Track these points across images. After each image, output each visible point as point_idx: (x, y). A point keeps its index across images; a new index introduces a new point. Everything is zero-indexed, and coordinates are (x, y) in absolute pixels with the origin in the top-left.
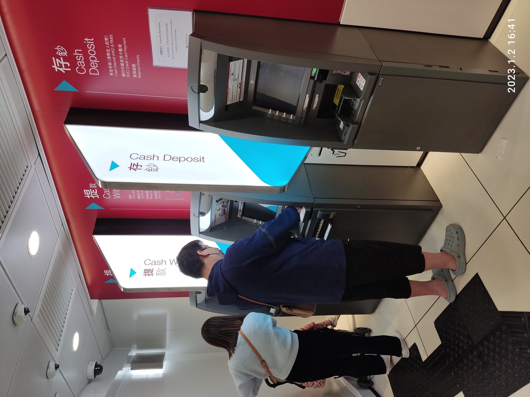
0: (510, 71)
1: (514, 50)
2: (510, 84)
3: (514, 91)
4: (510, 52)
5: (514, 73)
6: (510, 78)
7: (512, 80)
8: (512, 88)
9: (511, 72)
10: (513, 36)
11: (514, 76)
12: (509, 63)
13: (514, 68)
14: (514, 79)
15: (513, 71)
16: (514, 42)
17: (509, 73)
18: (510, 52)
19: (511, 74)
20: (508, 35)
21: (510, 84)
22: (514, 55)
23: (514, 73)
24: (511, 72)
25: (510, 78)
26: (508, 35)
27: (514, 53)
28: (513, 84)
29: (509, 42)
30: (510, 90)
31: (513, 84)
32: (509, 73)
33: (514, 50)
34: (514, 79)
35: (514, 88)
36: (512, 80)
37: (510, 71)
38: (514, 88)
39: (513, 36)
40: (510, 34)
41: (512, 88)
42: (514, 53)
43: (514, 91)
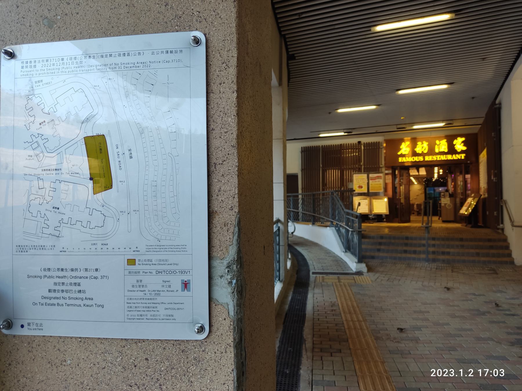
1: (473, 376)
2: (439, 372)
3: (432, 375)
4: (471, 371)
5: (450, 375)
6: (446, 371)
7: (444, 373)
8: (436, 374)
9: (451, 373)
11: (447, 376)
12: (460, 371)
13: (455, 375)
14: (444, 375)
15: (452, 374)
17: (450, 370)
18: (471, 371)
19: (449, 373)
21: (439, 372)
22: (468, 375)
23: (450, 375)
24: (451, 373)
25: (446, 371)
27: (470, 375)
28: (439, 374)
29: (480, 370)
30: (433, 371)
31: (439, 374)
32: (450, 370)
33: (473, 376)
34: (444, 375)
35: (435, 376)
36: (444, 373)
38: (435, 376)
41: (436, 374)
42: (470, 375)
43: (432, 375)
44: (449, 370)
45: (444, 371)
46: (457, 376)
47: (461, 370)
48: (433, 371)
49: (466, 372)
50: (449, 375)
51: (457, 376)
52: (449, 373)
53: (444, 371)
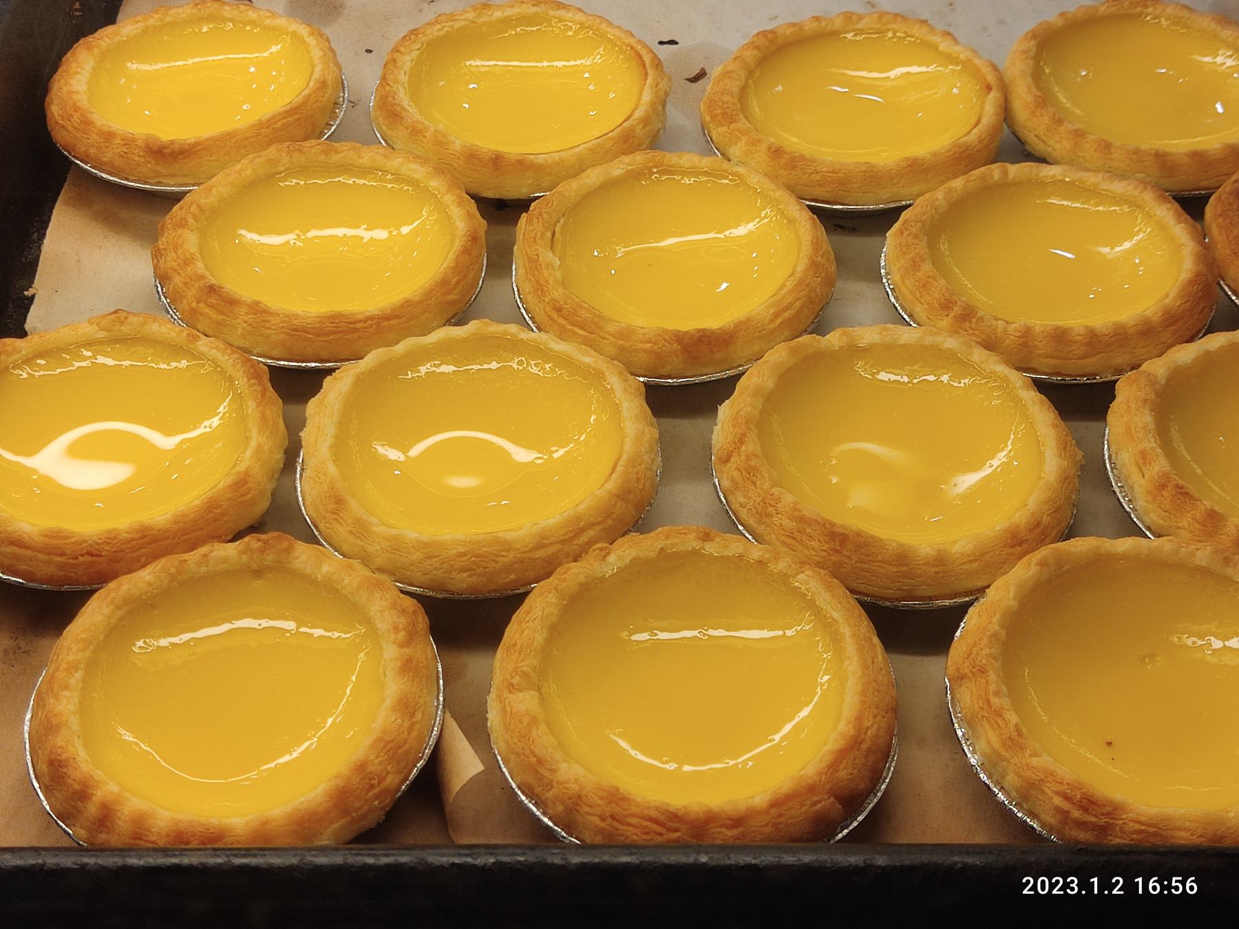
0: (1072, 882)
1: (1122, 893)
2: (1043, 882)
3: (1025, 892)
4: (1118, 882)
5: (1068, 891)
6: (1058, 882)
7: (1052, 886)
8: (1034, 888)
9: (1071, 885)
10: (1154, 888)
11: (1062, 893)
12: (1091, 880)
13: (1080, 891)
14: (1054, 892)
15: (1073, 889)
16: (1140, 892)
17: (1069, 880)
18: (1118, 882)
19: (1066, 886)
20: (1156, 878)
21: (1043, 882)
22: (1110, 892)
23: (1068, 891)
24: (1071, 885)
25: (1058, 882)
26: (1156, 878)
27: (1115, 892)
28: (1043, 889)
29: (1140, 880)
30: (1028, 882)
31: (1043, 889)
32: (1069, 880)
33: (1122, 893)
34: (1054, 892)
35: (1033, 893)
36: (1052, 886)
37: (1072, 882)
38: (1033, 893)
39: (1154, 888)
40: (1160, 881)
41: (1034, 888)
42: (1115, 892)
43: (1025, 892)
45: (1053, 881)
46: (1084, 892)
47: (1095, 880)
48: (1028, 882)
49: (1106, 884)
50: (1066, 892)
51: (1084, 892)
52: (1066, 886)
53: (1053, 881)
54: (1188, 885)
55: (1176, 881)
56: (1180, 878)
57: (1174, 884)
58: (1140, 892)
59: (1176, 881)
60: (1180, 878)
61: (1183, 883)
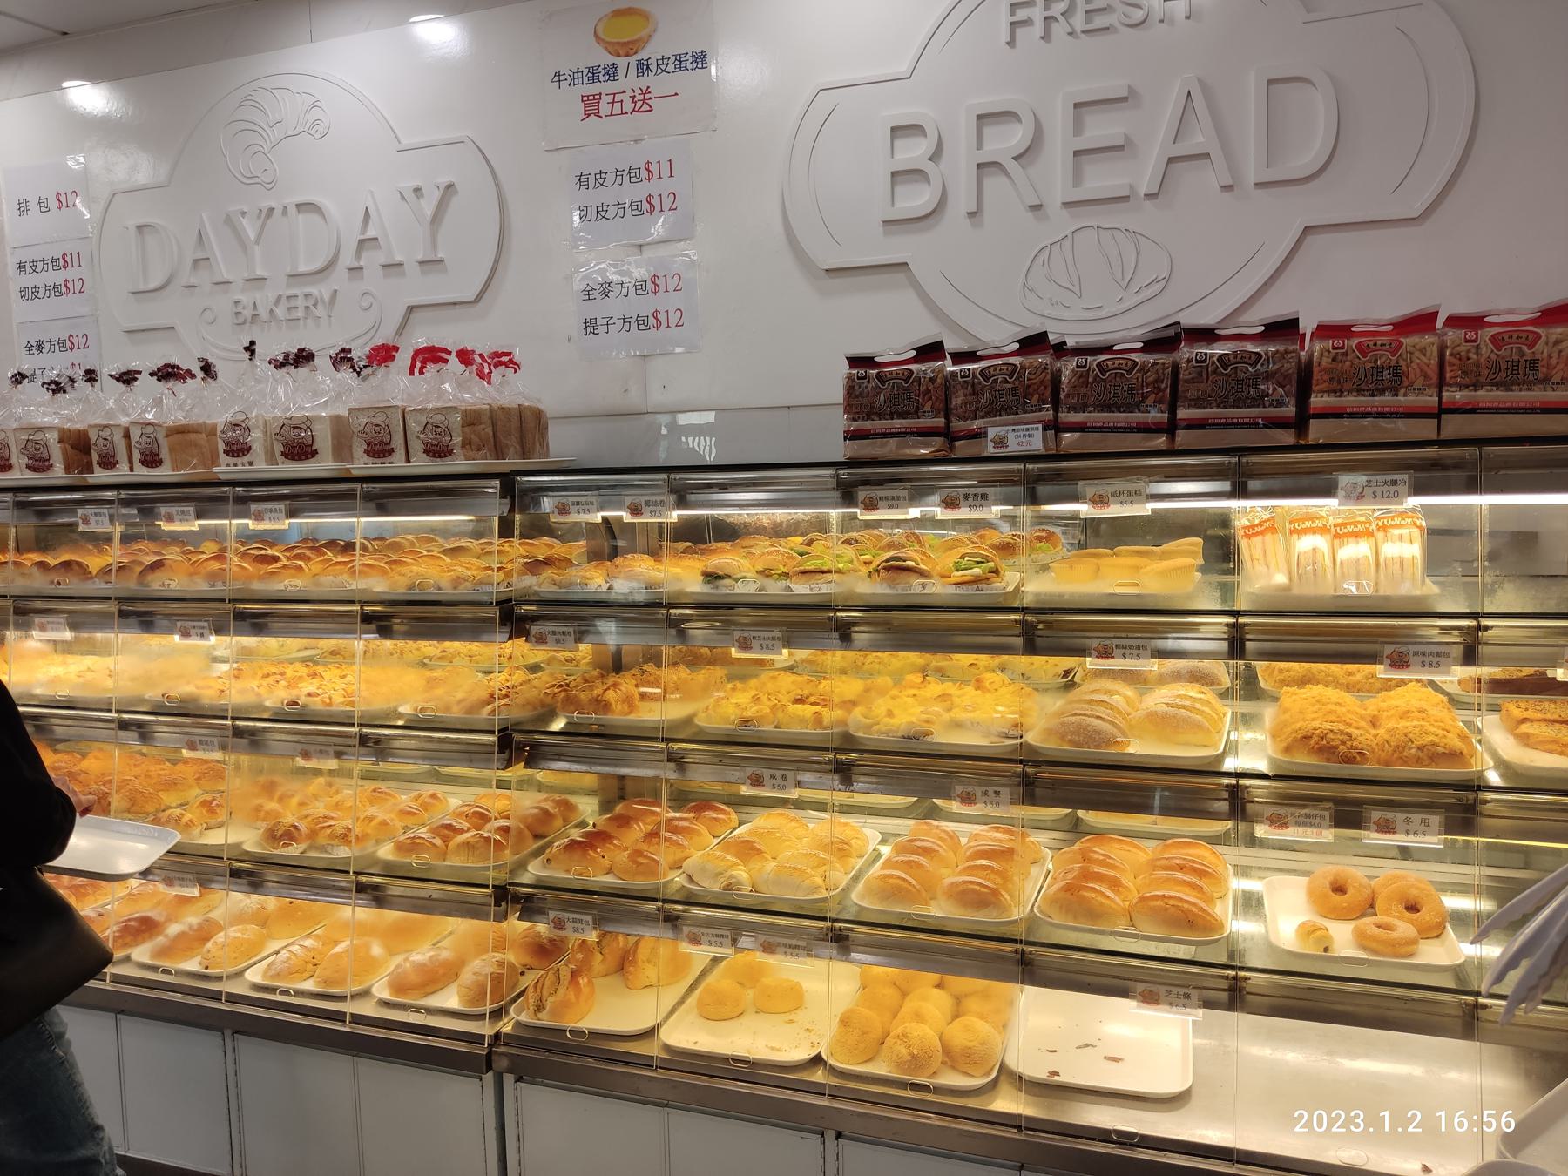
0: (1357, 1116)
2: (1320, 1116)
4: (1415, 1116)
5: (1352, 1128)
6: (1339, 1116)
7: (1331, 1124)
10: (1461, 1124)
12: (1381, 1114)
15: (1357, 1126)
16: (1443, 1129)
17: (1352, 1114)
18: (1415, 1116)
19: (1349, 1121)
21: (1320, 1116)
23: (1352, 1128)
25: (1339, 1116)
27: (1410, 1129)
29: (1443, 1114)
30: (1301, 1116)
32: (1352, 1114)
36: (1331, 1124)
37: (1357, 1116)
39: (1461, 1124)
41: (1309, 1124)
42: (1410, 1129)
44: (1347, 1114)
45: (1333, 1115)
46: (1371, 1130)
47: (1386, 1114)
48: (1301, 1116)
53: (1333, 1115)
54: (1503, 1120)
55: (1489, 1116)
56: (1494, 1112)
57: (1485, 1119)
58: (1443, 1129)
59: (1489, 1116)
60: (1494, 1112)
61: (1498, 1118)
